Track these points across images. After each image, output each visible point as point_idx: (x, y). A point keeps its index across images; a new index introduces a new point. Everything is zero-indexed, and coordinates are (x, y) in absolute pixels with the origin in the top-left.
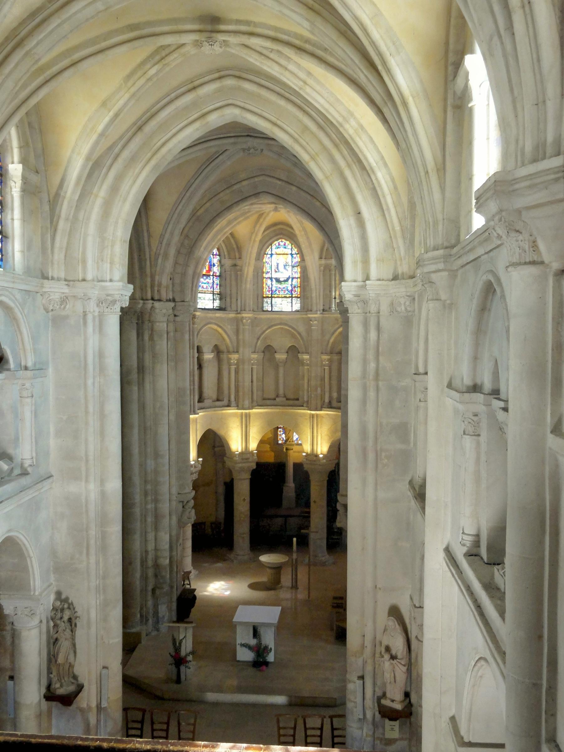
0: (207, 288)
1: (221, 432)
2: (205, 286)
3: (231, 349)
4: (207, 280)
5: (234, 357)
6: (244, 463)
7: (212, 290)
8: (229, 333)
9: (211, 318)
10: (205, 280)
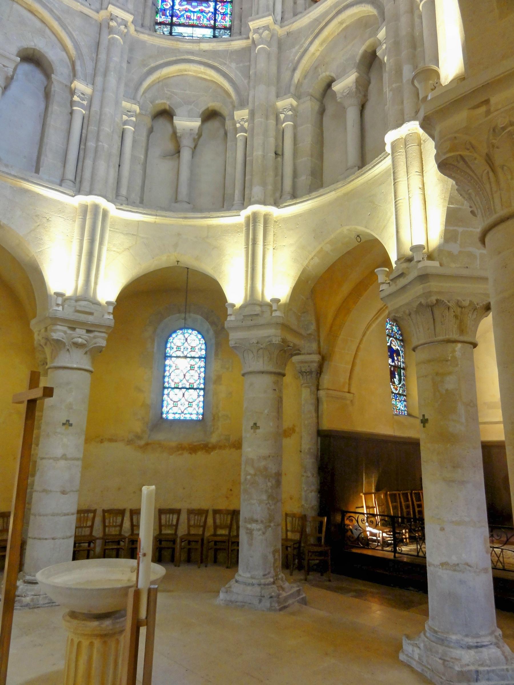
0: (199, 18)
1: (208, 268)
2: (194, 17)
3: (236, 104)
4: (200, 8)
5: (241, 115)
6: (249, 328)
7: (212, 22)
8: (232, 75)
9: (192, 53)
10: (194, 7)
